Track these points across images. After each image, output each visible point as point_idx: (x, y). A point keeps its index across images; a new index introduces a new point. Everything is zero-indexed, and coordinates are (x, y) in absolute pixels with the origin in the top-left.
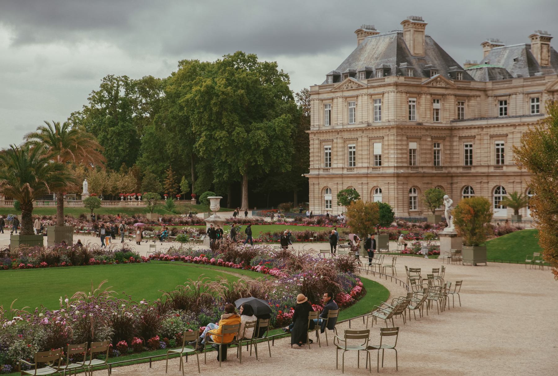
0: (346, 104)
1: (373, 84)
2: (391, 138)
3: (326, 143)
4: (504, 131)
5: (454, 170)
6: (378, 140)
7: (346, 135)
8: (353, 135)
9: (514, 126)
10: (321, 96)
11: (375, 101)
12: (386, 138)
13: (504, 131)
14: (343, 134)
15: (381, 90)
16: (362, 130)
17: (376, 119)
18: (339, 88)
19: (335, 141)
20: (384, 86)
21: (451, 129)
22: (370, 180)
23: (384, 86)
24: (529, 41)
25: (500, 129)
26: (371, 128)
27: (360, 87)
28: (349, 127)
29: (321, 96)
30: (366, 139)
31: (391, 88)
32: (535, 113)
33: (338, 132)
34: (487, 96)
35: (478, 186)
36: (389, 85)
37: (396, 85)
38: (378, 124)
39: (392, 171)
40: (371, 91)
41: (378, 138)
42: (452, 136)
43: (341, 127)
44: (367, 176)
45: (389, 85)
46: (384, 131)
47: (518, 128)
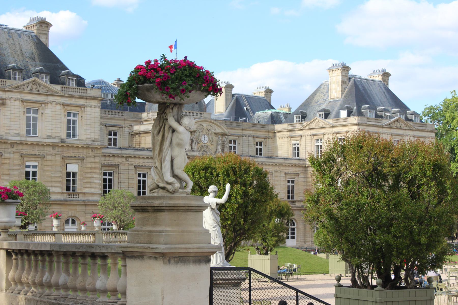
0: (25, 110)
1: (73, 93)
3: (29, 159)
4: (116, 161)
6: (74, 161)
7: (26, 150)
8: (38, 151)
9: (128, 157)
11: (69, 115)
13: (116, 161)
14: (20, 147)
16: (54, 146)
17: (68, 135)
19: (6, 155)
20: (87, 98)
23: (87, 99)
25: (112, 159)
26: (65, 145)
28: (29, 139)
30: (59, 158)
32: (112, 147)
33: (13, 144)
38: (71, 141)
40: (66, 101)
41: (76, 158)
43: (18, 138)
45: (95, 98)
46: (85, 151)
47: (130, 160)
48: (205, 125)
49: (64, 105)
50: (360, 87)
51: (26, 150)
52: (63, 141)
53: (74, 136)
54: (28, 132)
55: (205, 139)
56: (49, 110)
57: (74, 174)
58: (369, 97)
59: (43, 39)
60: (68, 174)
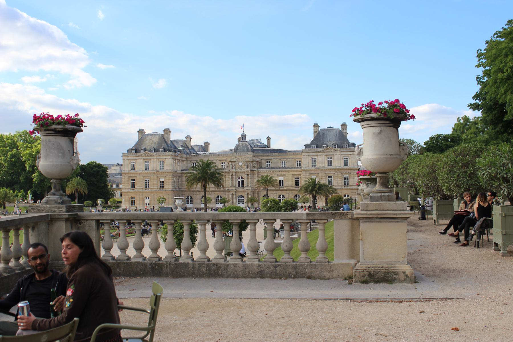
2: (170, 177)
5: (183, 189)
10: (129, 158)
12: (167, 177)
15: (164, 157)
16: (154, 173)
18: (141, 155)
20: (166, 156)
21: (182, 173)
22: (158, 193)
24: (185, 139)
27: (152, 155)
29: (129, 158)
31: (169, 157)
33: (140, 174)
34: (187, 161)
35: (195, 196)
36: (169, 155)
37: (172, 156)
38: (162, 171)
39: (170, 190)
42: (182, 176)
44: (157, 191)
45: (169, 155)
48: (240, 158)
49: (158, 159)
50: (321, 134)
51: (144, 175)
52: (157, 171)
53: (163, 169)
54: (146, 169)
55: (240, 164)
56: (152, 161)
57: (163, 182)
58: (323, 138)
59: (165, 136)
60: (161, 182)
